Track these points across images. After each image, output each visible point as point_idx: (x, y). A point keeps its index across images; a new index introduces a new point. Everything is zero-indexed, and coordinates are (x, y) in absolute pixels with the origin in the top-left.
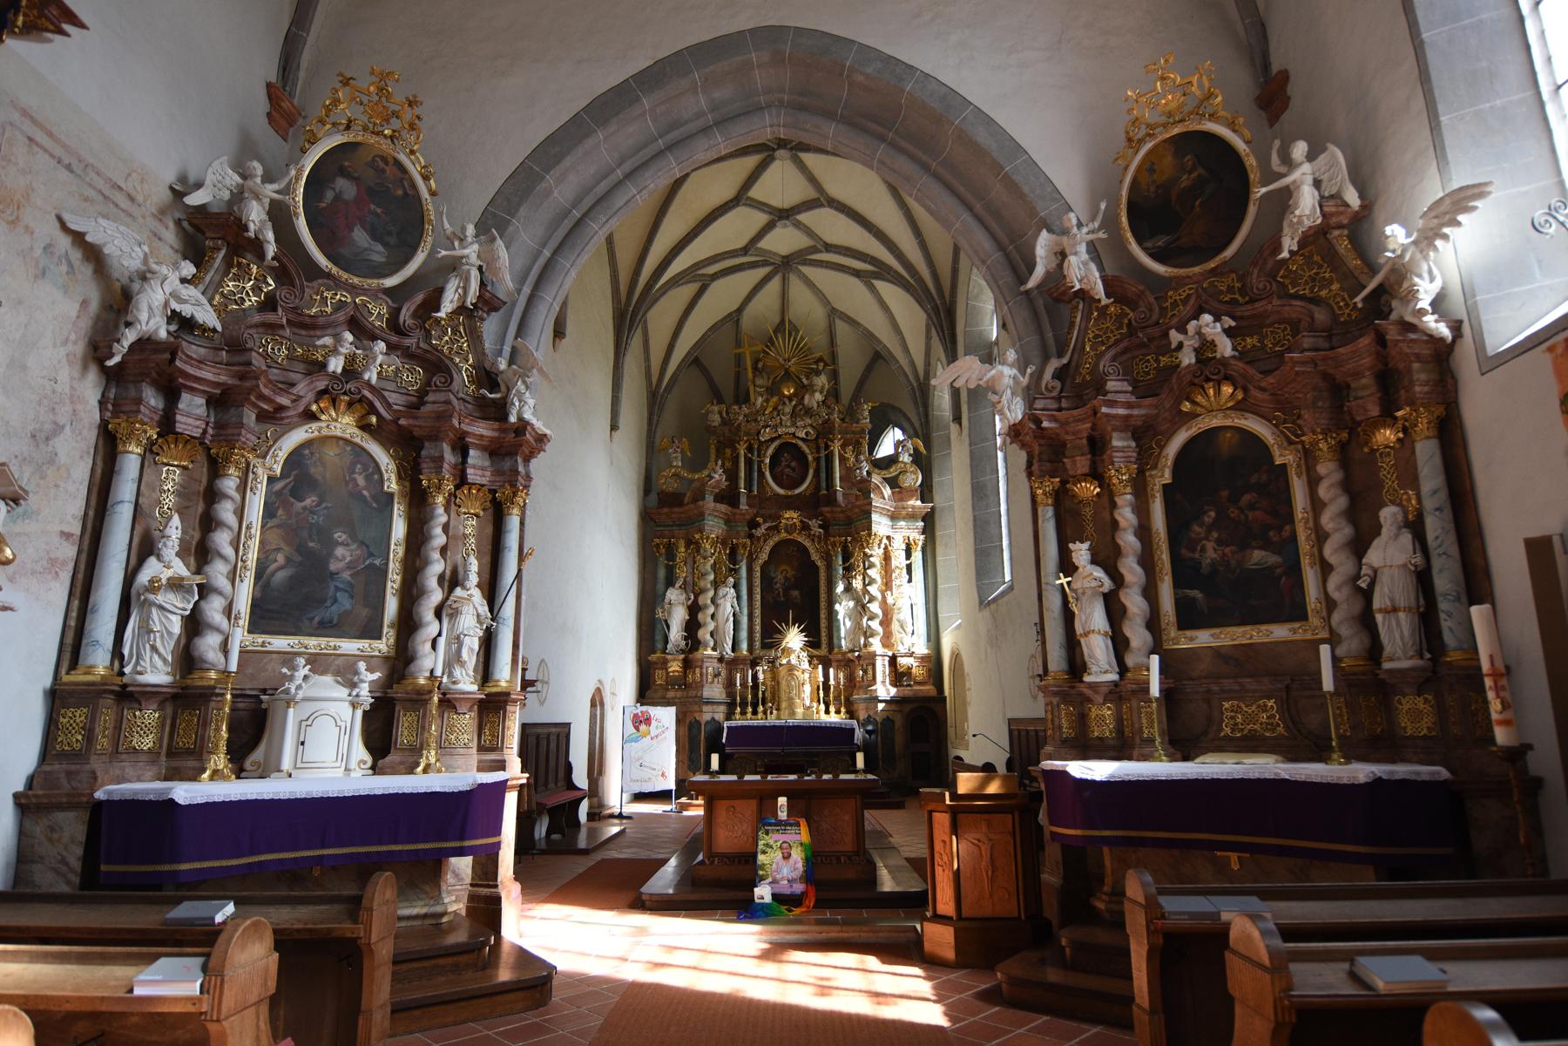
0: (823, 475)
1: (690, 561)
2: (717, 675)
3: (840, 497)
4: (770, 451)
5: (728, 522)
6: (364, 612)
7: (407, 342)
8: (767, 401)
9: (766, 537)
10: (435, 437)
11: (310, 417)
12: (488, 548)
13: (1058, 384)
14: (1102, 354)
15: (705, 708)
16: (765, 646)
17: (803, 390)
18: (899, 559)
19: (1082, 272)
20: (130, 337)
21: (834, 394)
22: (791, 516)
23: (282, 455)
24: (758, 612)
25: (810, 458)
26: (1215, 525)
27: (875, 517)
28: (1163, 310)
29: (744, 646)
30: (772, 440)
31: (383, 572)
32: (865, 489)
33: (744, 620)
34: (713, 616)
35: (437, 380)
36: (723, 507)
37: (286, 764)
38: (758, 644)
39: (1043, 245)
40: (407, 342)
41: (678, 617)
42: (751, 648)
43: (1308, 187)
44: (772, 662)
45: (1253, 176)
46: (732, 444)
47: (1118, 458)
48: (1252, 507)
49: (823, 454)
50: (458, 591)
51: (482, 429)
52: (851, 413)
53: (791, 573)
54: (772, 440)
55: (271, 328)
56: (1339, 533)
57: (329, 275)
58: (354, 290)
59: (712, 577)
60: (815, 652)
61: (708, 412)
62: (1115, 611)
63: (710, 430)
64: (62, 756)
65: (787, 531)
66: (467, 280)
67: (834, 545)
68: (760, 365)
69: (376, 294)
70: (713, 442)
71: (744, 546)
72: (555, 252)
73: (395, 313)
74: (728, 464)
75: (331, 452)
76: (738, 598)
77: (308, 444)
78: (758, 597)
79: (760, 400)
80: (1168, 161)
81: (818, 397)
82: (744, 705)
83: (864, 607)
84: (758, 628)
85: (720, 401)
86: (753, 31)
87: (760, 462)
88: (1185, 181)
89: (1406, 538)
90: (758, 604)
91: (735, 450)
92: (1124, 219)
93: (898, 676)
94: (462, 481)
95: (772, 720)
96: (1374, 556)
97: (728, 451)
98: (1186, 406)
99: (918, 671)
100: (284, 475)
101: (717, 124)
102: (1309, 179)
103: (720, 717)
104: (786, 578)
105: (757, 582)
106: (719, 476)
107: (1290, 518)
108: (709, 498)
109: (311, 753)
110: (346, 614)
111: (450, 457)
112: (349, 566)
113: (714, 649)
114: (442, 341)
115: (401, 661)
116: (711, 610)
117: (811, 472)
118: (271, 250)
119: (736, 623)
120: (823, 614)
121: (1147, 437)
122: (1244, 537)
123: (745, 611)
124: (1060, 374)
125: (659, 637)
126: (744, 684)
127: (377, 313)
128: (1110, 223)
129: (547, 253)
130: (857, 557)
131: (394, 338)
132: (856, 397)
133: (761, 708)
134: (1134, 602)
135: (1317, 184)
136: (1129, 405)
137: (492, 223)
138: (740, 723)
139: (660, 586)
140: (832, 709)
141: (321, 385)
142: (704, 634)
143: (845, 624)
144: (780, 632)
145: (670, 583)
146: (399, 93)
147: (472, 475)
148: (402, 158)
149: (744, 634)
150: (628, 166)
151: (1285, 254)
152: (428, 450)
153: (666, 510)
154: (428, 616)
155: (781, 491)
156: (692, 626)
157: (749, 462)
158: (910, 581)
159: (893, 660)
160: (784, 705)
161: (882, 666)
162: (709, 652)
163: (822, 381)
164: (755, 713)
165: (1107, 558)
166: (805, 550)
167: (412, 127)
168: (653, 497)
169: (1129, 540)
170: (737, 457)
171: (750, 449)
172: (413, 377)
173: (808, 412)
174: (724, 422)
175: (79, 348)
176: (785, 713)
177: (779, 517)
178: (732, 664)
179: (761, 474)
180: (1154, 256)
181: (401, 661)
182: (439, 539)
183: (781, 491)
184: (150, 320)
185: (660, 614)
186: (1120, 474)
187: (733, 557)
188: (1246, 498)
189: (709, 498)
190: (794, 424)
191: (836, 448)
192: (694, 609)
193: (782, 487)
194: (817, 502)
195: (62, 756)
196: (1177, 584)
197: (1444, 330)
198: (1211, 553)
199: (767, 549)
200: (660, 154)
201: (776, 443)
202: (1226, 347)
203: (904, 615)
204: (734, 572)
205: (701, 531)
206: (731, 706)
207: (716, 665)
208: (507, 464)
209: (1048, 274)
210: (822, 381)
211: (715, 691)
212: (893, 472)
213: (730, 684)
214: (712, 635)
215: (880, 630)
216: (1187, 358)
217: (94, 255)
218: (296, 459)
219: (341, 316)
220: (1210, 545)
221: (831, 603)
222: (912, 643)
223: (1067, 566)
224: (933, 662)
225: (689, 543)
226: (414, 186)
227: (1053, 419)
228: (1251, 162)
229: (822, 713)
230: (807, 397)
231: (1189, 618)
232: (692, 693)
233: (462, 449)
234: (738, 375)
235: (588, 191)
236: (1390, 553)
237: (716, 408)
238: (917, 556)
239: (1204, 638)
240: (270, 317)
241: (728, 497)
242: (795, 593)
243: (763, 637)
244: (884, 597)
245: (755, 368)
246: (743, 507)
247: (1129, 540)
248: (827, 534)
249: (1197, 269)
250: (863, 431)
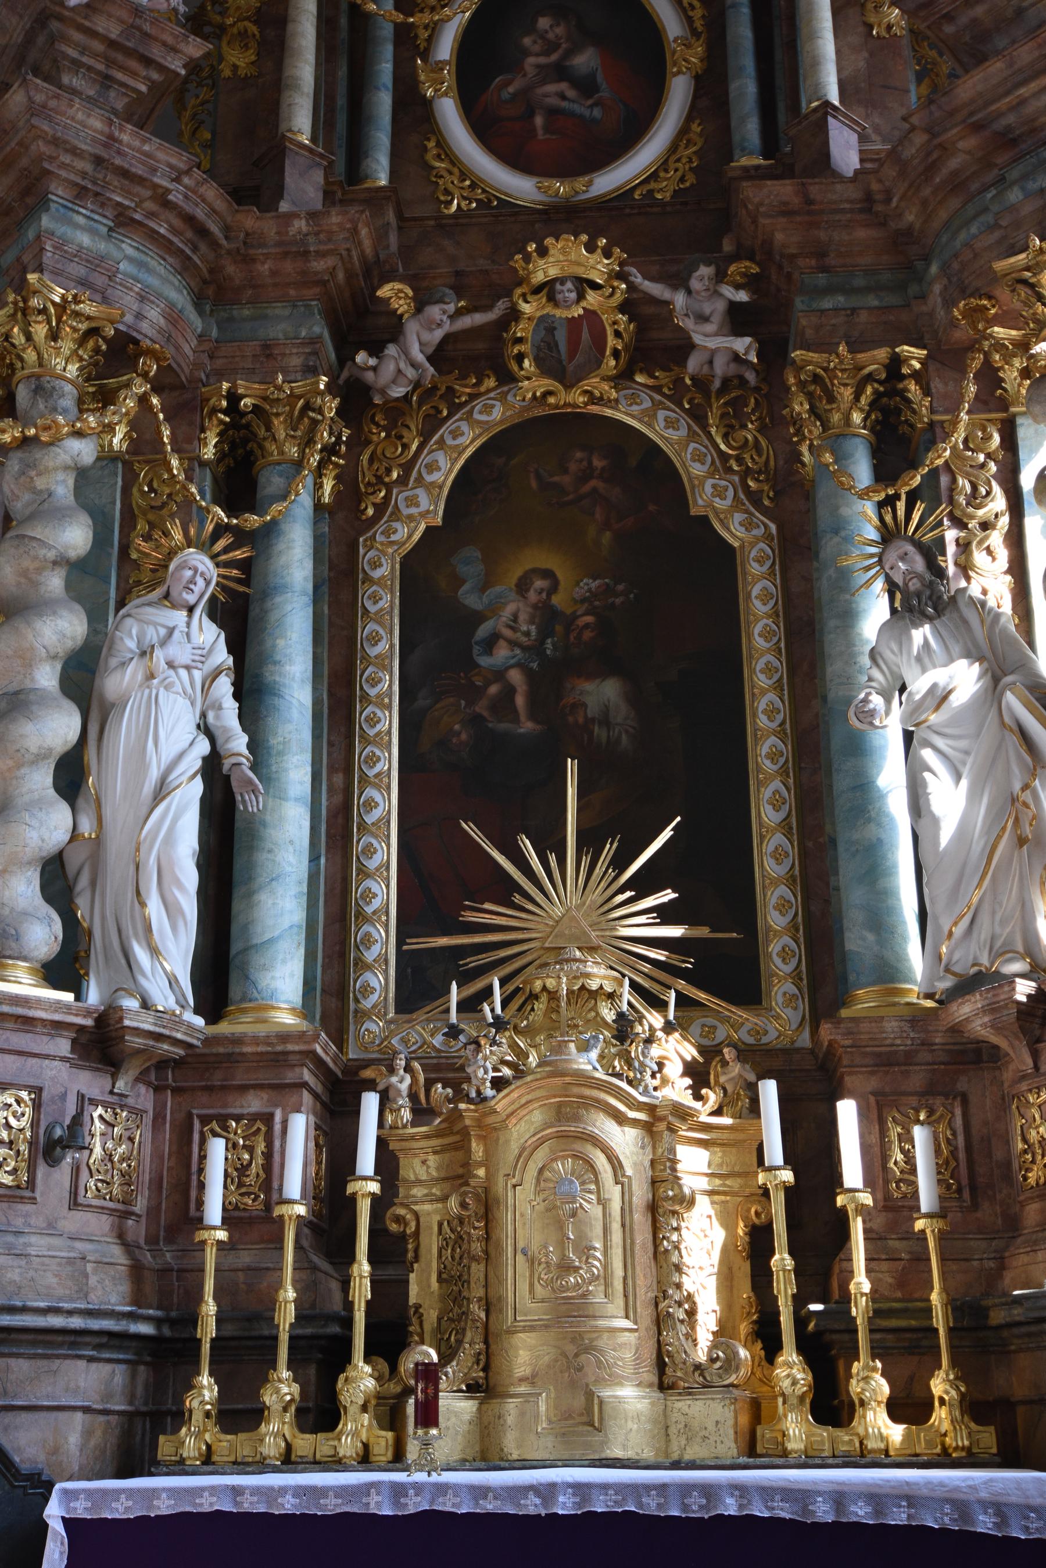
0: (745, 88)
3: (845, 150)
5: (212, 292)
9: (433, 406)
24: (384, 804)
29: (282, 982)
38: (379, 984)
53: (573, 589)
59: (76, 537)
65: (551, 364)
76: (252, 691)
78: (390, 722)
82: (244, 1356)
84: (382, 893)
87: (411, 45)
95: (441, 1474)
104: (548, 617)
105: (383, 641)
113: (64, 970)
117: (679, 92)
123: (297, 771)
126: (254, 1221)
133: (362, 1379)
138: (208, 1491)
140: (871, 1383)
144: (504, 891)
155: (520, 187)
160: (525, 1354)
164: (321, 1413)
166: (650, 472)
176: (530, 1415)
179: (414, 115)
183: (520, 187)
187: (240, 482)
199: (444, 469)
206: (165, 1357)
207: (68, 1080)
214: (58, 879)
229: (796, 1428)
242: (602, 694)
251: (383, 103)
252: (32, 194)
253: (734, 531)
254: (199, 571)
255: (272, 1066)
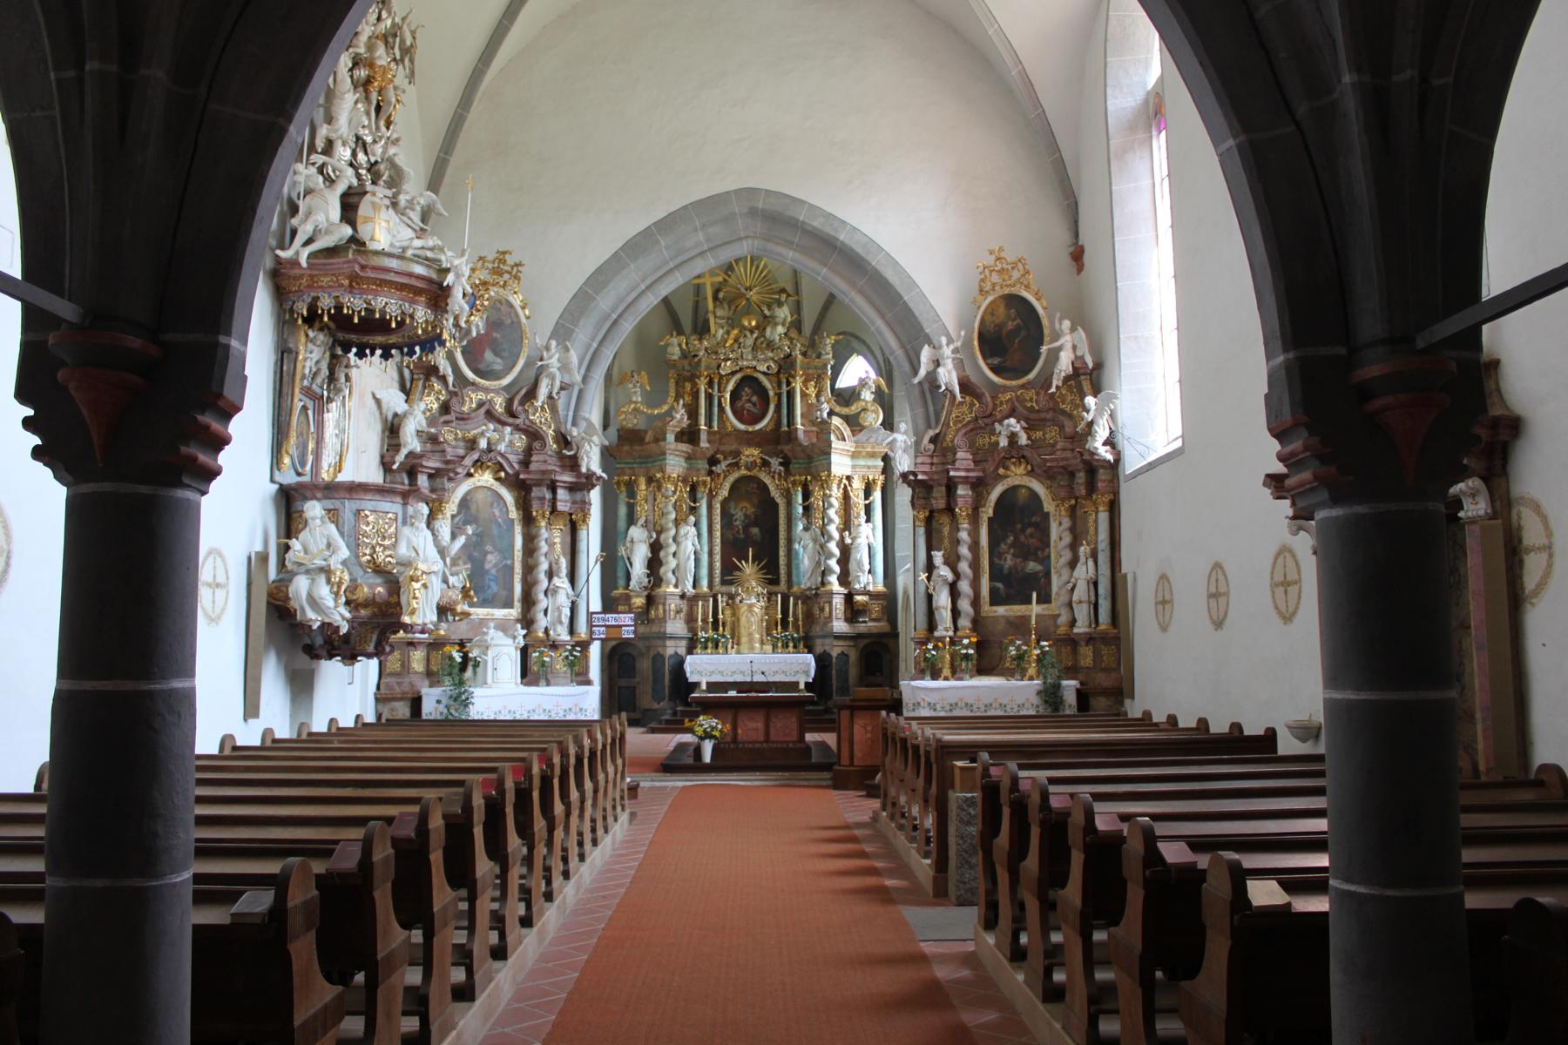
0: (785, 411)
1: (650, 498)
2: (678, 612)
3: (801, 435)
4: (730, 387)
5: (689, 458)
6: (504, 593)
7: (518, 421)
8: (728, 333)
9: (727, 474)
10: (539, 483)
11: (470, 475)
12: (568, 550)
13: (932, 447)
14: (958, 430)
15: (669, 643)
16: (723, 582)
17: (766, 321)
18: (858, 499)
19: (948, 376)
20: (404, 452)
21: (797, 325)
22: (751, 453)
23: (457, 501)
24: (718, 549)
25: (771, 393)
26: (1012, 545)
27: (834, 458)
28: (995, 406)
29: (704, 583)
30: (733, 373)
31: (512, 568)
32: (823, 428)
33: (705, 558)
34: (674, 554)
35: (537, 445)
36: (685, 447)
37: (489, 680)
38: (717, 580)
39: (926, 354)
40: (518, 421)
41: (640, 554)
42: (711, 585)
43: (1066, 350)
44: (731, 597)
45: (1046, 331)
46: (693, 378)
47: (960, 502)
48: (1031, 536)
49: (785, 389)
50: (556, 580)
51: (567, 478)
52: (812, 348)
54: (733, 373)
55: (447, 423)
56: (1067, 555)
57: (473, 384)
58: (486, 390)
59: (673, 516)
60: (775, 589)
61: (667, 345)
62: (954, 594)
63: (671, 365)
64: (391, 674)
65: (747, 468)
66: (553, 379)
67: (794, 483)
68: (721, 295)
69: (497, 392)
70: (672, 374)
71: (704, 483)
72: (601, 343)
73: (509, 402)
74: (688, 399)
75: (480, 496)
76: (699, 535)
77: (469, 493)
78: (718, 534)
79: (721, 332)
80: (1001, 310)
81: (780, 329)
83: (822, 546)
84: (718, 565)
85: (680, 332)
86: (736, 191)
88: (1011, 325)
89: (1091, 563)
90: (718, 541)
91: (695, 385)
92: (976, 343)
93: (853, 611)
94: (554, 510)
96: (1076, 573)
97: (688, 386)
98: (1001, 471)
99: (876, 608)
100: (459, 513)
101: (710, 249)
102: (1069, 346)
103: (682, 651)
104: (746, 516)
105: (717, 519)
106: (681, 415)
107: (1048, 545)
108: (671, 437)
109: (500, 673)
110: (494, 595)
111: (548, 496)
112: (495, 566)
113: (676, 586)
114: (536, 418)
115: (527, 621)
116: (673, 548)
117: (772, 407)
118: (450, 379)
119: (697, 560)
120: (782, 552)
121: (979, 486)
122: (1026, 553)
123: (706, 549)
124: (933, 440)
125: (621, 573)
127: (499, 404)
128: (967, 343)
129: (595, 345)
130: (817, 493)
131: (511, 420)
132: (818, 328)
134: (964, 586)
135: (1074, 348)
136: (967, 470)
137: (562, 332)
139: (622, 522)
141: (476, 456)
142: (666, 572)
143: (805, 561)
144: (739, 569)
145: (631, 520)
146: (510, 260)
147: (561, 506)
148: (511, 299)
149: (704, 572)
150: (648, 282)
151: (1053, 390)
152: (536, 492)
153: (626, 448)
154: (541, 596)
156: (654, 564)
157: (709, 397)
158: (868, 521)
159: (849, 598)
160: (744, 640)
161: (838, 602)
162: (671, 589)
163: (784, 313)
165: (952, 562)
166: (765, 488)
167: (517, 278)
168: (613, 431)
169: (964, 550)
170: (698, 392)
171: (710, 384)
172: (520, 441)
173: (770, 345)
174: (684, 355)
175: (378, 459)
177: (737, 454)
178: (692, 600)
179: (721, 409)
180: (994, 370)
181: (527, 621)
182: (544, 548)
184: (411, 442)
185: (622, 551)
186: (962, 509)
188: (1029, 530)
189: (671, 437)
190: (754, 358)
191: (798, 385)
192: (656, 547)
193: (741, 420)
194: (779, 440)
195: (391, 674)
196: (991, 579)
197: (1110, 457)
198: (1009, 561)
199: (727, 486)
200: (671, 270)
201: (739, 376)
202: (1023, 440)
203: (861, 555)
204: (693, 510)
205: (662, 470)
207: (678, 601)
208: (578, 496)
209: (928, 373)
210: (784, 313)
211: (676, 627)
212: (854, 409)
213: (690, 620)
215: (837, 569)
216: (1004, 442)
217: (378, 402)
218: (464, 503)
219: (483, 410)
220: (1009, 557)
221: (790, 541)
222: (869, 580)
223: (930, 567)
224: (888, 600)
225: (650, 480)
226: (517, 315)
227: (924, 473)
228: (1045, 322)
230: (768, 330)
231: (996, 599)
232: (655, 629)
233: (553, 488)
234: (696, 304)
235: (622, 300)
236: (1083, 572)
237: (675, 340)
238: (877, 496)
239: (1001, 610)
240: (447, 418)
241: (689, 435)
242: (755, 531)
243: (723, 574)
244: (842, 538)
245: (715, 298)
246: (704, 444)
247: (964, 550)
248: (788, 473)
249: (1014, 383)
250: (825, 366)
251: (716, 409)
252: (664, 454)
253: (779, 500)
254: (692, 519)
255: (704, 597)
